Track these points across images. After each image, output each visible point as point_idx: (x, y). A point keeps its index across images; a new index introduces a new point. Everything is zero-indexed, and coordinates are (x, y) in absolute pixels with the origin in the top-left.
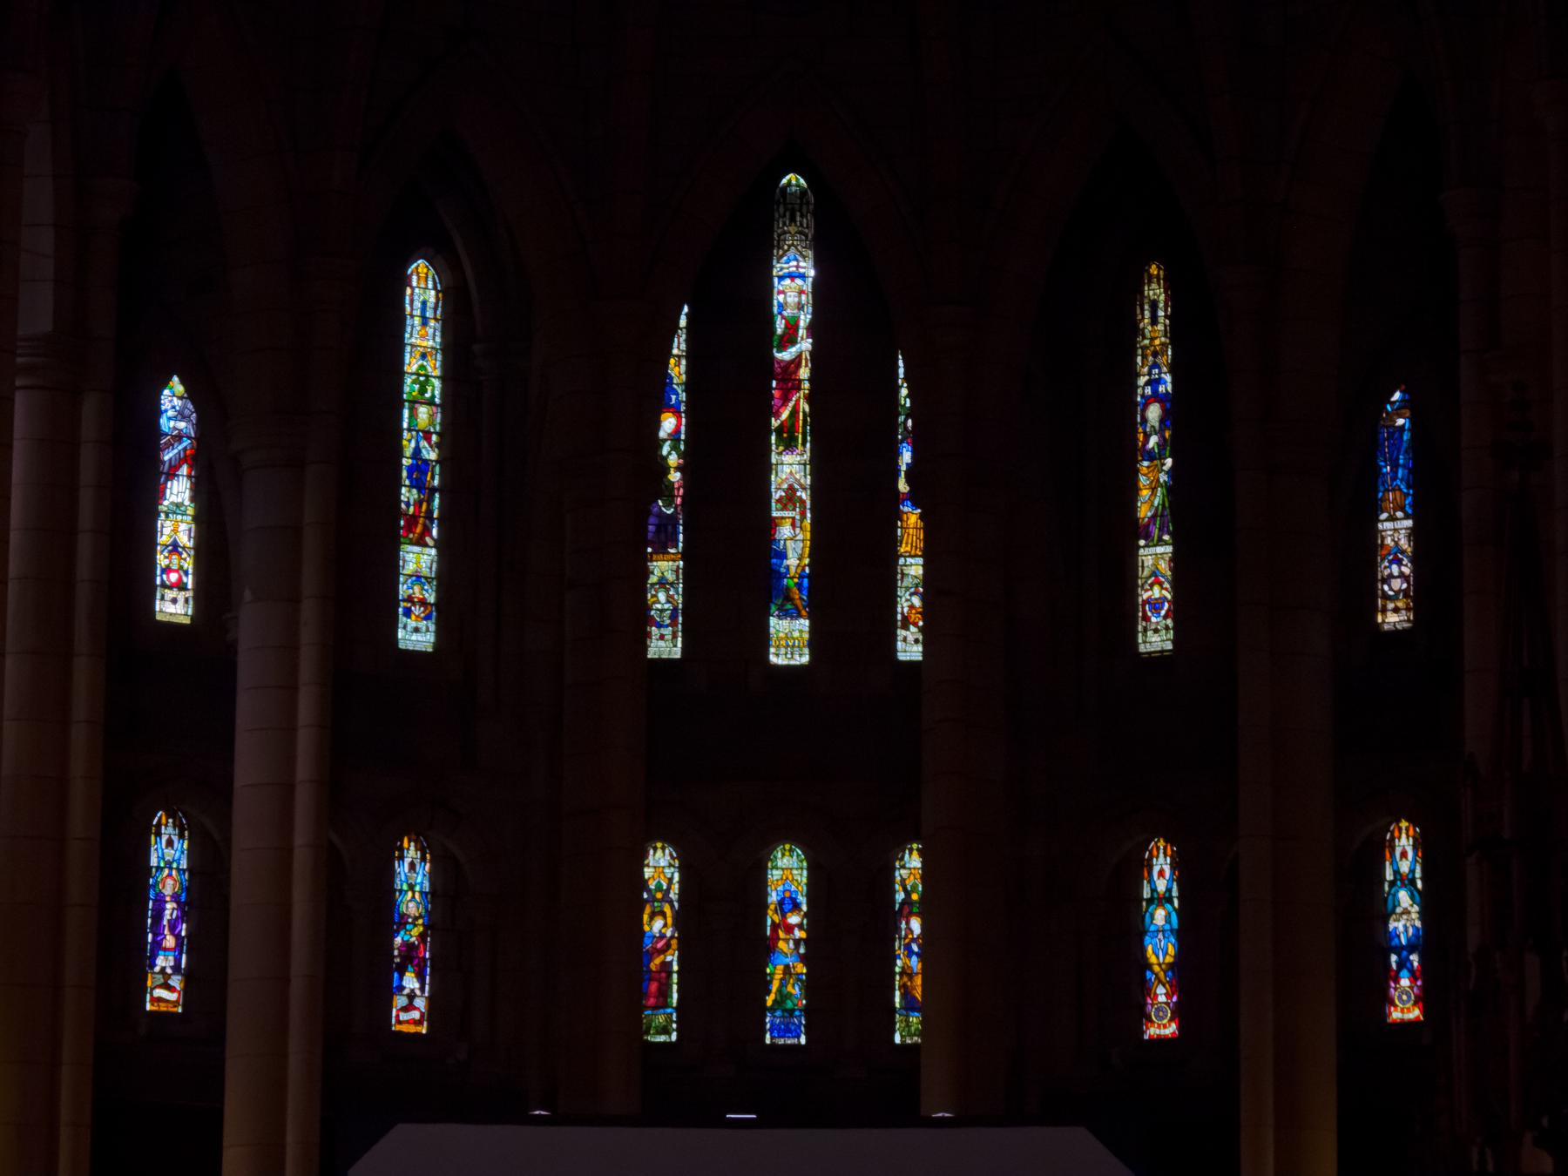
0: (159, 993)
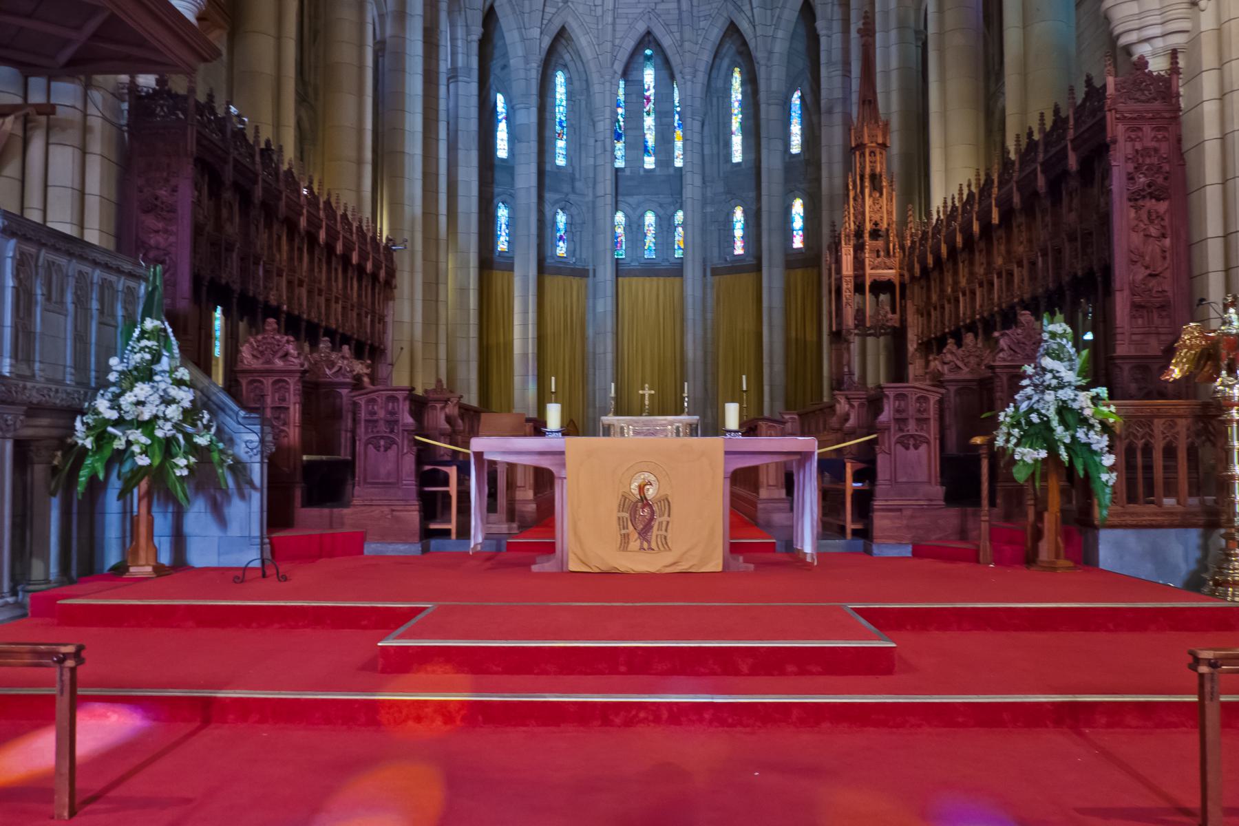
0: (502, 246)
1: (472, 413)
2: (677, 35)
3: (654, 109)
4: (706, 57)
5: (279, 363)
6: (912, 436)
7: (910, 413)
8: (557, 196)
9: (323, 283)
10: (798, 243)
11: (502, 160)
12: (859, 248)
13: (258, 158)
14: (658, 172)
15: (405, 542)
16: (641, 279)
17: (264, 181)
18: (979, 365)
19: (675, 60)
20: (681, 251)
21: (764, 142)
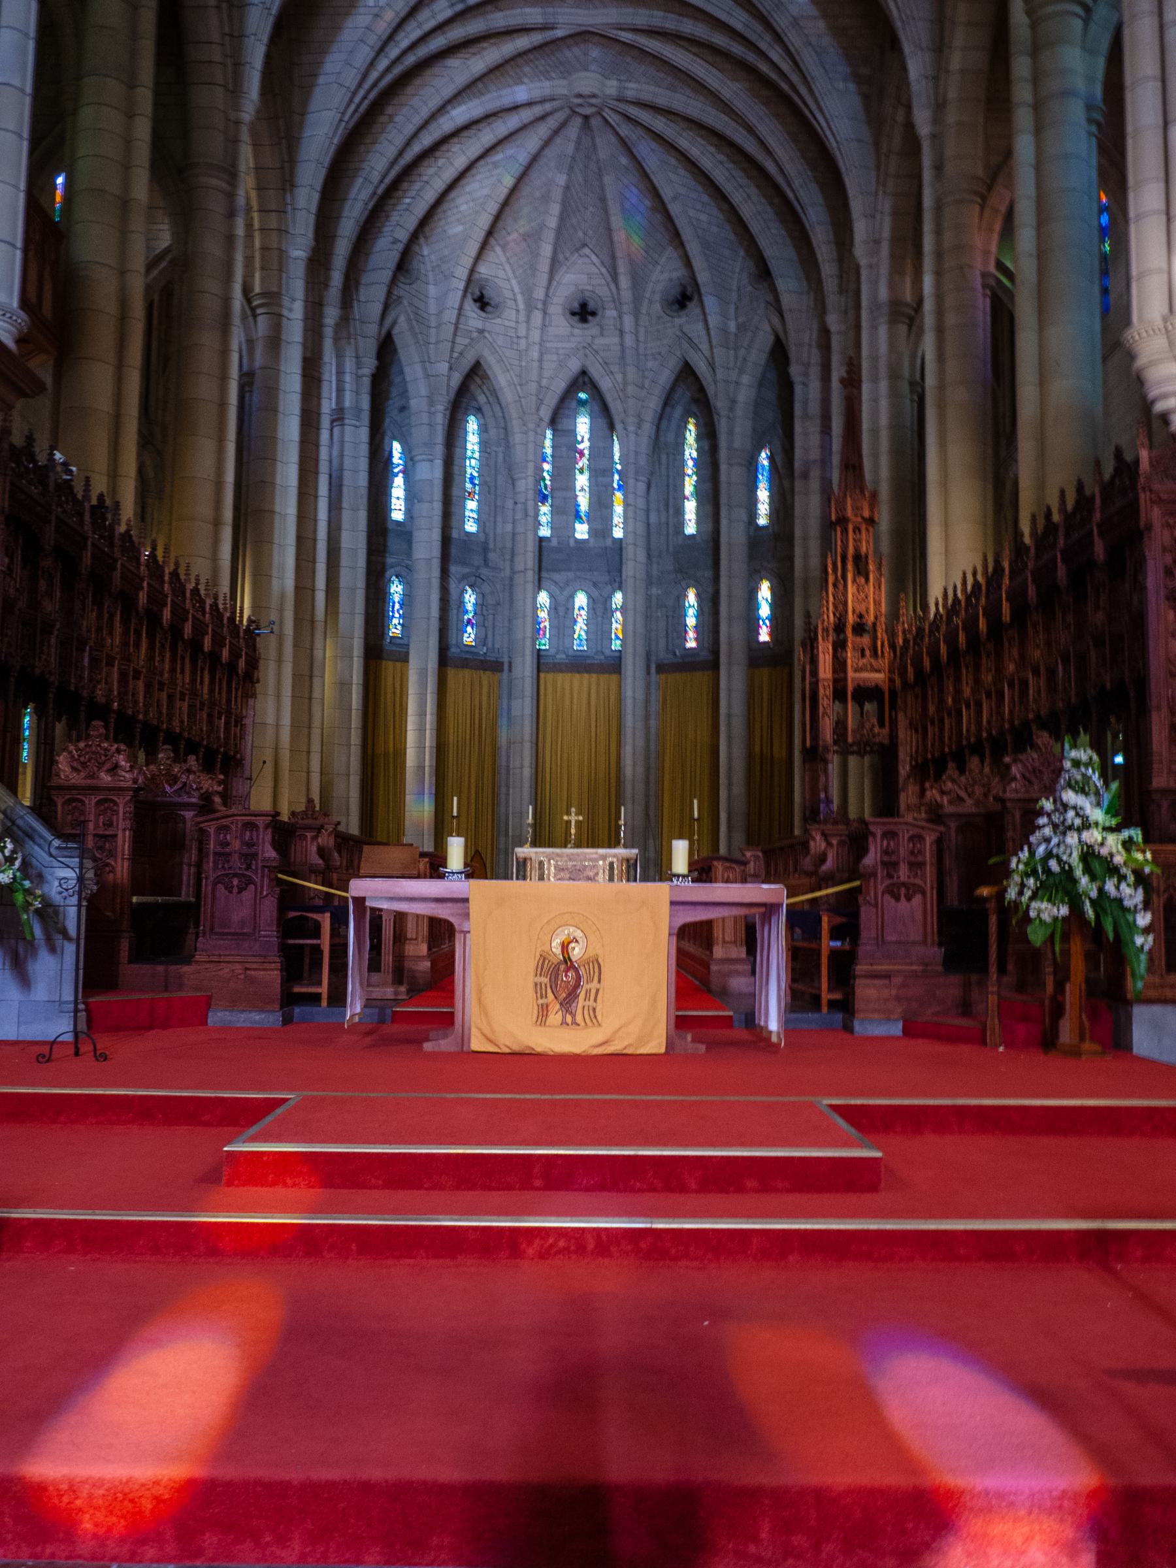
0: (394, 630)
1: (351, 843)
2: (619, 377)
3: (589, 467)
4: (654, 404)
5: (105, 778)
6: (904, 884)
7: (902, 855)
8: (466, 570)
9: (166, 675)
10: (764, 636)
11: (397, 523)
12: (839, 646)
13: (87, 517)
14: (592, 543)
15: (262, 1011)
16: (568, 676)
17: (93, 544)
18: (986, 795)
19: (616, 407)
20: (618, 642)
21: (724, 512)
